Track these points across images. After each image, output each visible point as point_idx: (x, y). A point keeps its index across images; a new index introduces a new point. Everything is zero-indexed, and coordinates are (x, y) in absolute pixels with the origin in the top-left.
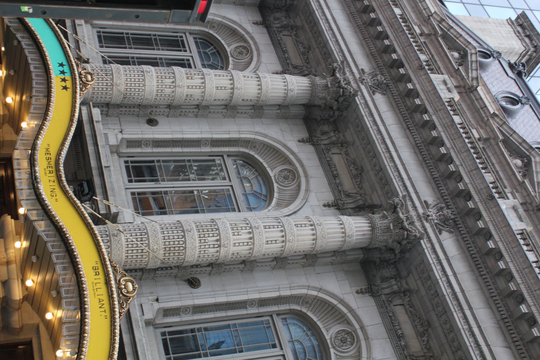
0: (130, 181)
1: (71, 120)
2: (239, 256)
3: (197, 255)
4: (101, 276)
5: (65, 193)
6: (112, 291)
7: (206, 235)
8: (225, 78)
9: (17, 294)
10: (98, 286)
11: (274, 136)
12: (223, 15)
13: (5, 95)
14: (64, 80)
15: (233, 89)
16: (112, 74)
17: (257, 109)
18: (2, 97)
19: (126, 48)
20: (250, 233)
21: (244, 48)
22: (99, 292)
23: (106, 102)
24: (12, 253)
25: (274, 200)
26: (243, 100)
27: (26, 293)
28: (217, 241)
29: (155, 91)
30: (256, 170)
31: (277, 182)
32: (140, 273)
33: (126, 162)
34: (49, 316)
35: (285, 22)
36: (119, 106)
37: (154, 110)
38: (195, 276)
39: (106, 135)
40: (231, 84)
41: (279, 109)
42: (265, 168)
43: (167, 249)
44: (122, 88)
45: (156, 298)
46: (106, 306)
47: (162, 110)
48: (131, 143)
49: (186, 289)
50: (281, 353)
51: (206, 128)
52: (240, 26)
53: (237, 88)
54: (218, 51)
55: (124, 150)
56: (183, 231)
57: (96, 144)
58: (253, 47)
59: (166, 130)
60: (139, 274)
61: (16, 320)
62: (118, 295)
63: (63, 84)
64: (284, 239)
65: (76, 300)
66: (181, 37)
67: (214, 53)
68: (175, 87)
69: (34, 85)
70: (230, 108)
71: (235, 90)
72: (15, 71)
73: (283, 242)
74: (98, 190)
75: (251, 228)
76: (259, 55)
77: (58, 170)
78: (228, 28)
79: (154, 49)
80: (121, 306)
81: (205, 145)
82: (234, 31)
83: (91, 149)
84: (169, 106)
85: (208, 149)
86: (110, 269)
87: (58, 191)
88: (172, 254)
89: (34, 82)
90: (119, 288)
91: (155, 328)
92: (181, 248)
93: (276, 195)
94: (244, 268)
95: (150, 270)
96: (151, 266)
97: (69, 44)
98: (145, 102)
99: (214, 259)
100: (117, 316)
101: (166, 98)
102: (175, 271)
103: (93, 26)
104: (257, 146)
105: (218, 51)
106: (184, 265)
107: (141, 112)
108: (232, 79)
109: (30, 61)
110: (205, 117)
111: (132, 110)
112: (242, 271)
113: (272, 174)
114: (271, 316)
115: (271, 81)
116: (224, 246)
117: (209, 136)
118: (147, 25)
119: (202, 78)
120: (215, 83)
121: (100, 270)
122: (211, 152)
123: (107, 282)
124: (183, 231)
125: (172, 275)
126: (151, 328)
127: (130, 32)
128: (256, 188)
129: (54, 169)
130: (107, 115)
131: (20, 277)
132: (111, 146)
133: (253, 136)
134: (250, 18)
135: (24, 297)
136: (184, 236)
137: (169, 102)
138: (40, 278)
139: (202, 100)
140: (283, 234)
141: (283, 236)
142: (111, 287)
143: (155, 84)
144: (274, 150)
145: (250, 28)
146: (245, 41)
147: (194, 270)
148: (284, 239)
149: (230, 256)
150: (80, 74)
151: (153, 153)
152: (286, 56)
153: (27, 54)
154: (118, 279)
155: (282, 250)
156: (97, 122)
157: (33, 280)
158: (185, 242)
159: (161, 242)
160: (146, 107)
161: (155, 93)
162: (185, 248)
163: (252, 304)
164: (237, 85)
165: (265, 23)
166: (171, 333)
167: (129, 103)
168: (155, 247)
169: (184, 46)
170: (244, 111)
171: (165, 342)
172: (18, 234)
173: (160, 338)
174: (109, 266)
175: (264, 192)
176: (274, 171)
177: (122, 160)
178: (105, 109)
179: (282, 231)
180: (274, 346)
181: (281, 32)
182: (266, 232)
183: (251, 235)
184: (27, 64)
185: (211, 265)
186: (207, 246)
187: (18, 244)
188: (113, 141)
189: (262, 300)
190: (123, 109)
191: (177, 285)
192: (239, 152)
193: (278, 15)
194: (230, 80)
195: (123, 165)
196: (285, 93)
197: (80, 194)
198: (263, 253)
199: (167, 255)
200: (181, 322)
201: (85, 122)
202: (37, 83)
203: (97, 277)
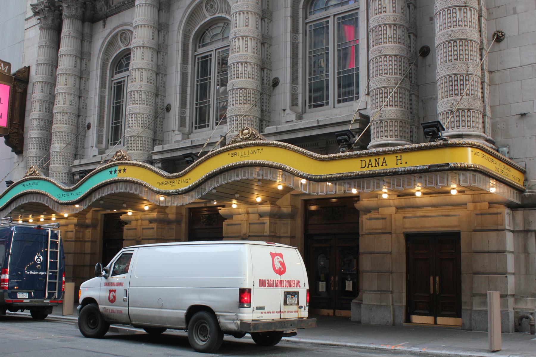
0: (208, 126)
1: (144, 167)
2: (256, 48)
3: (252, 80)
4: (238, 151)
5: (186, 173)
6: (246, 144)
7: (237, 72)
8: (135, 53)
9: (267, 208)
10: (243, 154)
11: (181, 15)
12: (98, 51)
13: (144, 211)
14: (120, 171)
15: (143, 47)
16: (131, 136)
17: (161, 28)
18: (146, 213)
19: (121, 125)
20: (239, 39)
21: (121, 35)
22: (246, 153)
23: (152, 141)
24: (241, 210)
25: (227, 17)
26: (153, 39)
27: (268, 202)
28: (242, 64)
29: (144, 106)
30: (207, 30)
31: (215, 14)
32: (264, 122)
33: (196, 128)
34: (280, 187)
35: (103, 2)
36: (155, 132)
37: (159, 106)
38: (271, 81)
39: (175, 142)
40: (140, 48)
41: (162, 10)
42: (205, 23)
43: (245, 102)
44: (141, 129)
45: (282, 111)
46: (255, 149)
47: (160, 100)
48: (182, 123)
49: (279, 88)
50: (332, 17)
51: (174, 67)
52: (106, 38)
53: (143, 44)
54: (125, 56)
55: (187, 129)
56: (233, 90)
57: (177, 150)
58: (120, 29)
59: (174, 98)
60: (264, 123)
61: (286, 210)
62: (250, 140)
63: (122, 171)
64: (245, 12)
65: (246, 169)
66: (115, 83)
67: (126, 59)
68: (141, 91)
69: (127, 191)
70: (160, 49)
71: (145, 45)
72: (124, 203)
73: (248, 13)
74: (194, 151)
75: (235, 38)
76: (126, 25)
77: (172, 178)
78: (108, 47)
79: (123, 105)
80: (257, 139)
81: (186, 69)
82: (110, 43)
83: (179, 154)
84: (157, 95)
85: (190, 67)
86: (233, 145)
87: (185, 178)
88: (249, 99)
89: (121, 191)
90: (246, 139)
91: (305, 112)
92: (245, 91)
93: (223, 15)
94: (268, 44)
95: (262, 115)
96: (258, 114)
97: (98, 167)
98: (153, 113)
99: (256, 67)
100: (262, 141)
101: (150, 97)
102: (265, 97)
103: (107, 148)
104: (189, 28)
105: (125, 56)
106: (259, 89)
107: (161, 116)
108: (137, 47)
109: (109, 193)
110: (166, 69)
111: (158, 123)
112: (271, 45)
113: (209, 18)
114: (306, 23)
115: (139, 17)
116: (246, 59)
117: (179, 66)
118: (106, 109)
119: (135, 71)
120: (140, 60)
121: (234, 152)
122: (192, 64)
123: (241, 147)
124: (233, 90)
125: (268, 98)
126: (304, 116)
127: (111, 122)
128: (218, 31)
129: (172, 180)
130: (162, 141)
131: (257, 205)
132: (183, 139)
133: (181, 32)
134: (101, 30)
135: (271, 204)
136: (237, 89)
137: (152, 95)
138: (256, 193)
139: (152, 70)
140: (241, 13)
141: (244, 13)
142: (244, 145)
143: (138, 106)
144: (191, 15)
145: (107, 31)
146: (117, 34)
147: (265, 82)
148: (245, 12)
149: (255, 55)
150: (117, 160)
151: (190, 108)
152: (126, 2)
153: (104, 195)
154: (240, 140)
155: (255, 14)
156: (163, 149)
157: (257, 197)
158: (241, 89)
159: (239, 106)
160: (156, 112)
161: (146, 106)
162: (245, 89)
163: (295, 38)
164: (140, 44)
165: (104, 18)
166: (310, 102)
167: (153, 124)
168: (243, 111)
169: (121, 82)
170: (163, 38)
171: (315, 106)
172: (230, 206)
173: (313, 109)
174: (231, 146)
175: (222, 24)
176: (207, 16)
177: (194, 131)
178: (157, 142)
179: (240, 14)
180: (328, 22)
181: (110, 6)
182: (239, 26)
183: (240, 38)
184: (114, 194)
185: (262, 69)
186: (246, 72)
187: (234, 206)
188: (179, 137)
189: (293, 31)
190: (158, 129)
191: (275, 95)
192: (193, 43)
193: (98, 8)
194: (137, 49)
195: (198, 130)
196: (149, 6)
197: (189, 163)
198: (256, 29)
199: (249, 102)
200: (302, 93)
201: (163, 157)
202: (121, 189)
203: (237, 155)
